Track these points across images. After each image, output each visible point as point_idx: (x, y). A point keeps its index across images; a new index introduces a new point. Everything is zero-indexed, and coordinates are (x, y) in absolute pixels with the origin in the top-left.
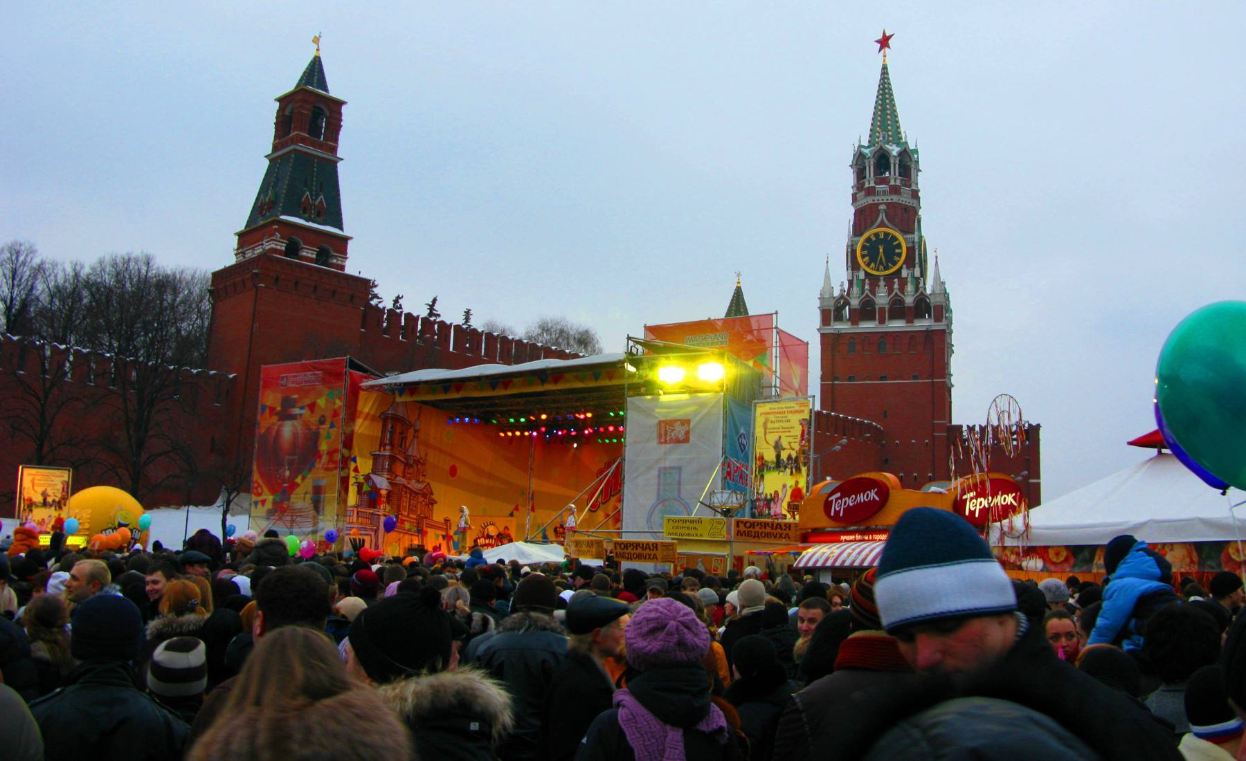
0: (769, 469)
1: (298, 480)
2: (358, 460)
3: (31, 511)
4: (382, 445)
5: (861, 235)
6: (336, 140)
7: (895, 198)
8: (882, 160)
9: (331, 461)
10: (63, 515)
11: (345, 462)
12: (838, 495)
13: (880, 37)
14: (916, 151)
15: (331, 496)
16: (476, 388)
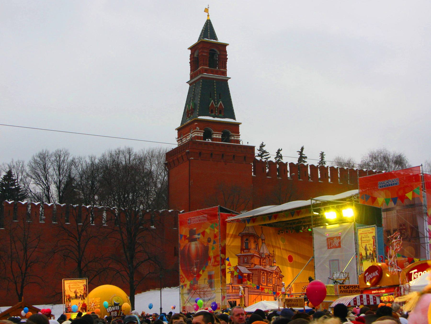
0: (364, 260)
1: (201, 273)
2: (230, 259)
3: (70, 301)
4: (242, 250)
6: (225, 67)
9: (216, 261)
10: (86, 302)
11: (223, 261)
12: (367, 273)
15: (217, 280)
16: (284, 216)
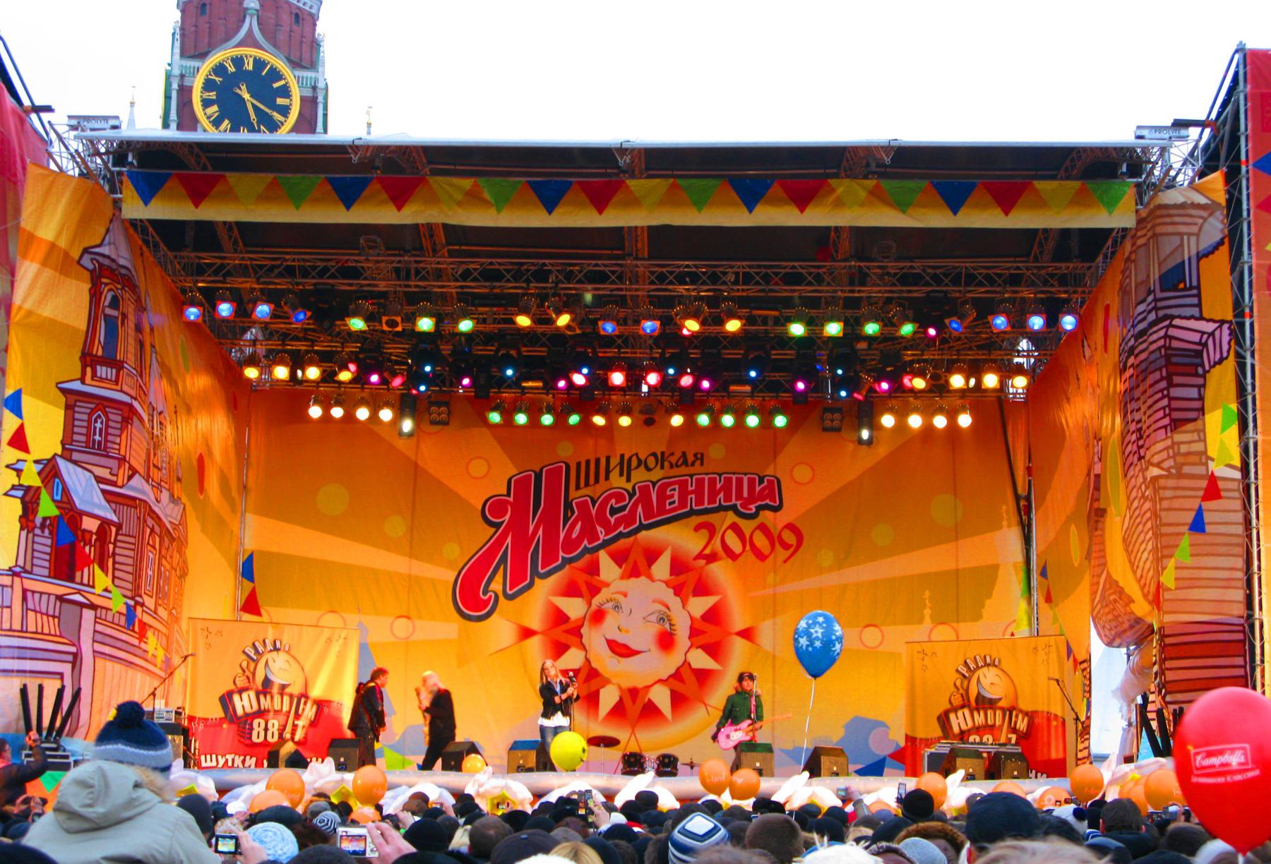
2: (27, 402)
4: (88, 360)
5: (203, 56)
16: (473, 197)
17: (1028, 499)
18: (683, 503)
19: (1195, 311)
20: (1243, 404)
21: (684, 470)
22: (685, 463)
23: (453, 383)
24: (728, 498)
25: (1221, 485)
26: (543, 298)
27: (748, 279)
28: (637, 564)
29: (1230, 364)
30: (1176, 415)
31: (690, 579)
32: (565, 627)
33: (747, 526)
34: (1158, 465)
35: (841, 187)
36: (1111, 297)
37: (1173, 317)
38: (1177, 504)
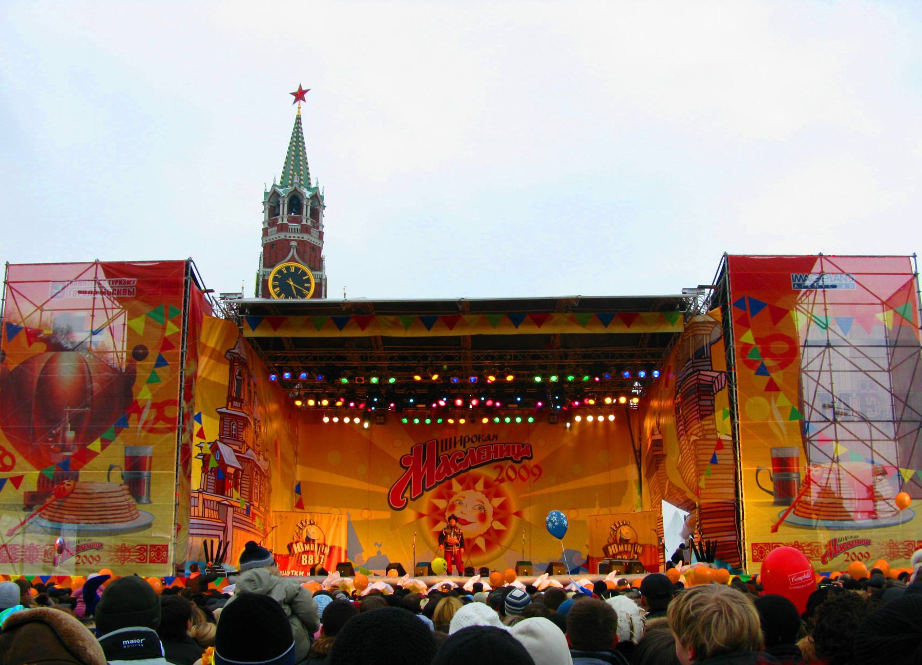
2: (203, 417)
4: (230, 399)
5: (272, 267)
7: (306, 237)
8: (295, 202)
9: (160, 417)
13: (296, 90)
14: (322, 197)
16: (395, 325)
17: (640, 451)
18: (488, 457)
19: (709, 368)
20: (732, 408)
21: (488, 442)
22: (489, 439)
23: (385, 406)
24: (508, 454)
25: (724, 443)
26: (426, 367)
27: (516, 357)
28: (469, 484)
29: (726, 390)
30: (702, 413)
31: (493, 490)
32: (493, 493)
33: (517, 466)
34: (696, 435)
35: (556, 316)
36: (672, 363)
37: (700, 370)
38: (704, 451)
